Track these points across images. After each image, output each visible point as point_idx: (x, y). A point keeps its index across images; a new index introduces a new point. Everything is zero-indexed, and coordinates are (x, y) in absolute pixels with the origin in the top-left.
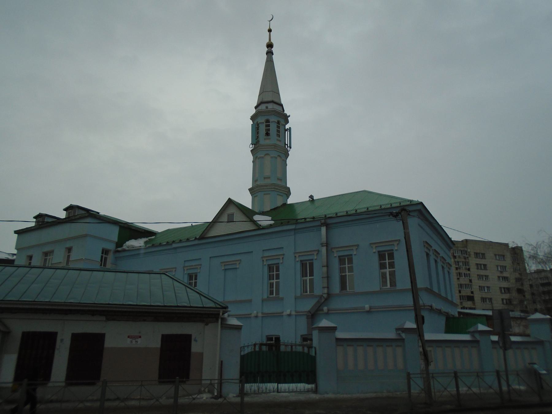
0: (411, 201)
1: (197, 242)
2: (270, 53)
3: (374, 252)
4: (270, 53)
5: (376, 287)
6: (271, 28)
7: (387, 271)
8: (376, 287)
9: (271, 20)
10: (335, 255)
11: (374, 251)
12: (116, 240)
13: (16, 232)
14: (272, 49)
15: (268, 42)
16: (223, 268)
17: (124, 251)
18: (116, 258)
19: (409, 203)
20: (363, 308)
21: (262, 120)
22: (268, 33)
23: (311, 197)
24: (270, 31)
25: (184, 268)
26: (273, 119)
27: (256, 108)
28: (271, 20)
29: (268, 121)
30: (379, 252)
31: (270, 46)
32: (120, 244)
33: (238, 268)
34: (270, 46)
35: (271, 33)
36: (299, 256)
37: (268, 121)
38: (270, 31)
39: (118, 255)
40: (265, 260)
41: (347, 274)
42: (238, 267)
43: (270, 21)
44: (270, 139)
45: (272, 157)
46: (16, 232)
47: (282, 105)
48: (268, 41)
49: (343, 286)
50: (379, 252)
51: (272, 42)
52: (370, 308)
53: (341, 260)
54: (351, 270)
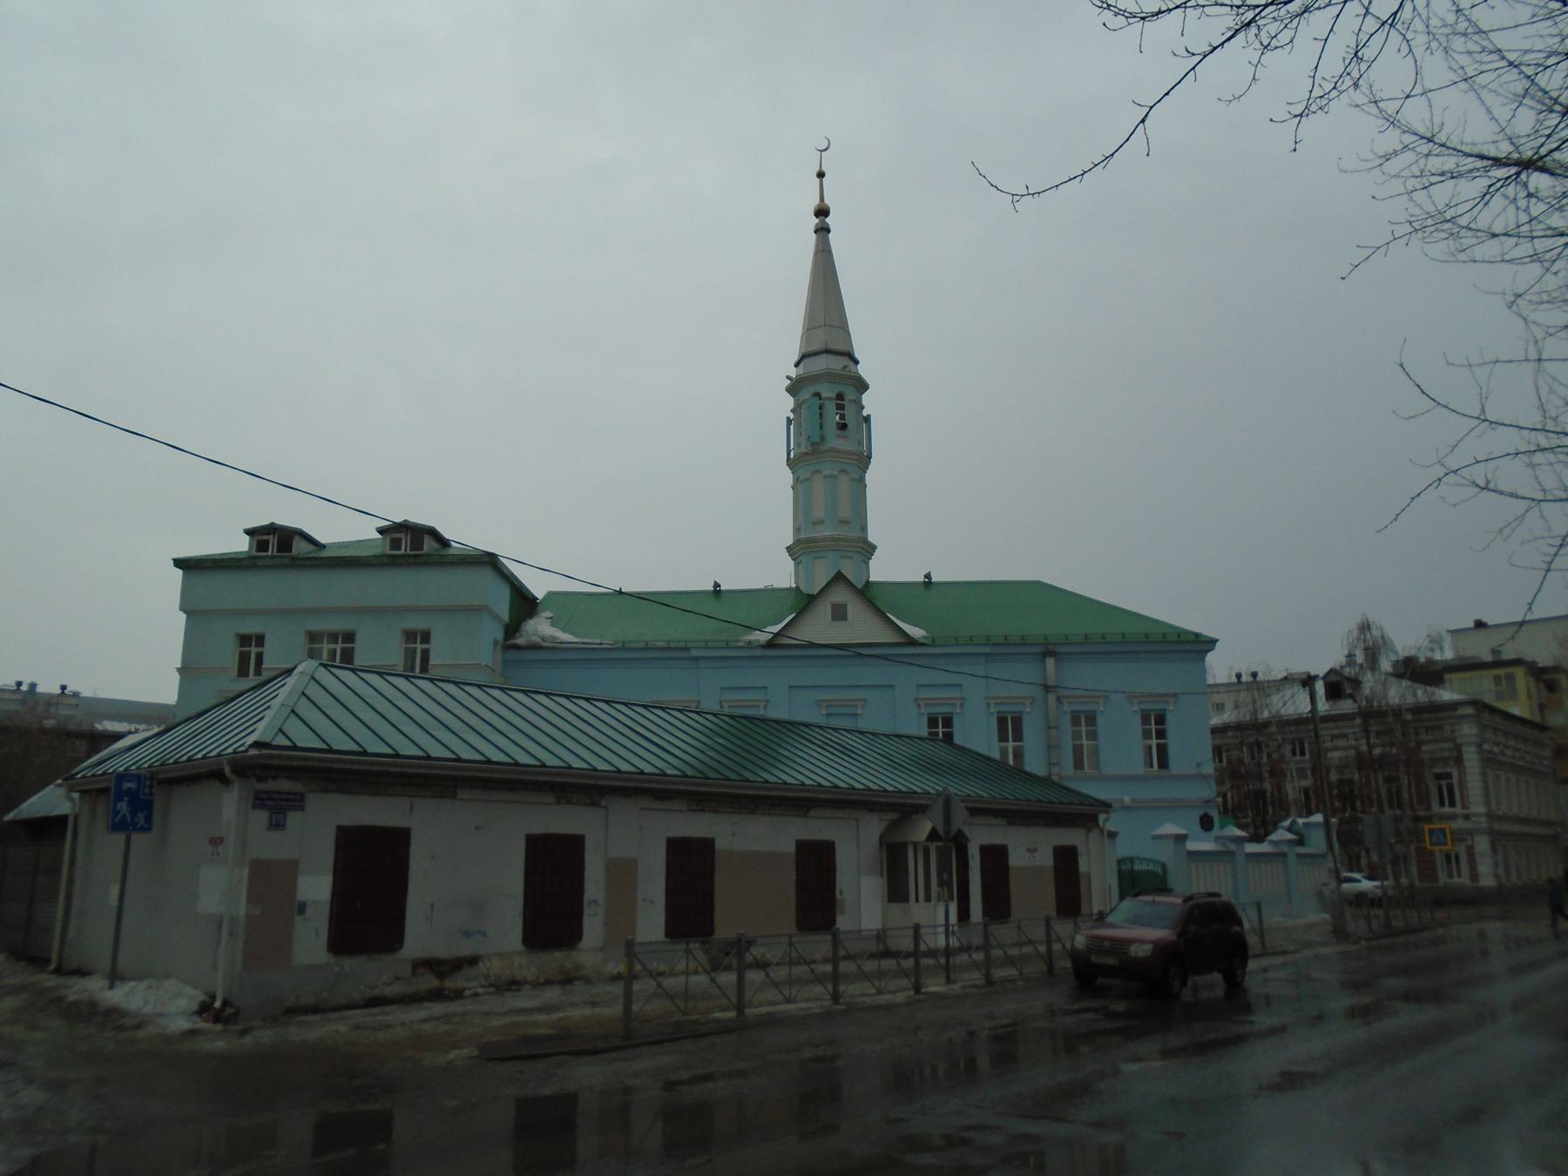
0: (1197, 635)
1: (758, 652)
2: (823, 231)
3: (1135, 711)
4: (823, 231)
5: (1140, 769)
6: (823, 168)
7: (1154, 742)
8: (1140, 769)
9: (826, 149)
10: (1066, 709)
11: (1136, 709)
12: (506, 617)
13: (179, 563)
14: (827, 220)
15: (819, 205)
16: (824, 712)
17: (535, 647)
18: (504, 661)
19: (1192, 638)
20: (1122, 801)
21: (828, 391)
22: (818, 180)
23: (928, 576)
24: (821, 175)
25: (721, 704)
26: (850, 394)
27: (804, 357)
28: (826, 149)
29: (840, 397)
30: (1142, 710)
31: (822, 212)
32: (512, 629)
33: (860, 715)
34: (822, 212)
35: (824, 180)
36: (996, 704)
37: (840, 397)
38: (821, 175)
39: (514, 655)
40: (922, 704)
41: (1085, 742)
42: (860, 712)
43: (821, 151)
44: (846, 437)
45: (853, 480)
46: (179, 563)
47: (856, 362)
48: (818, 202)
49: (1078, 764)
50: (1142, 710)
51: (826, 205)
52: (1133, 801)
53: (1075, 720)
54: (1093, 736)
